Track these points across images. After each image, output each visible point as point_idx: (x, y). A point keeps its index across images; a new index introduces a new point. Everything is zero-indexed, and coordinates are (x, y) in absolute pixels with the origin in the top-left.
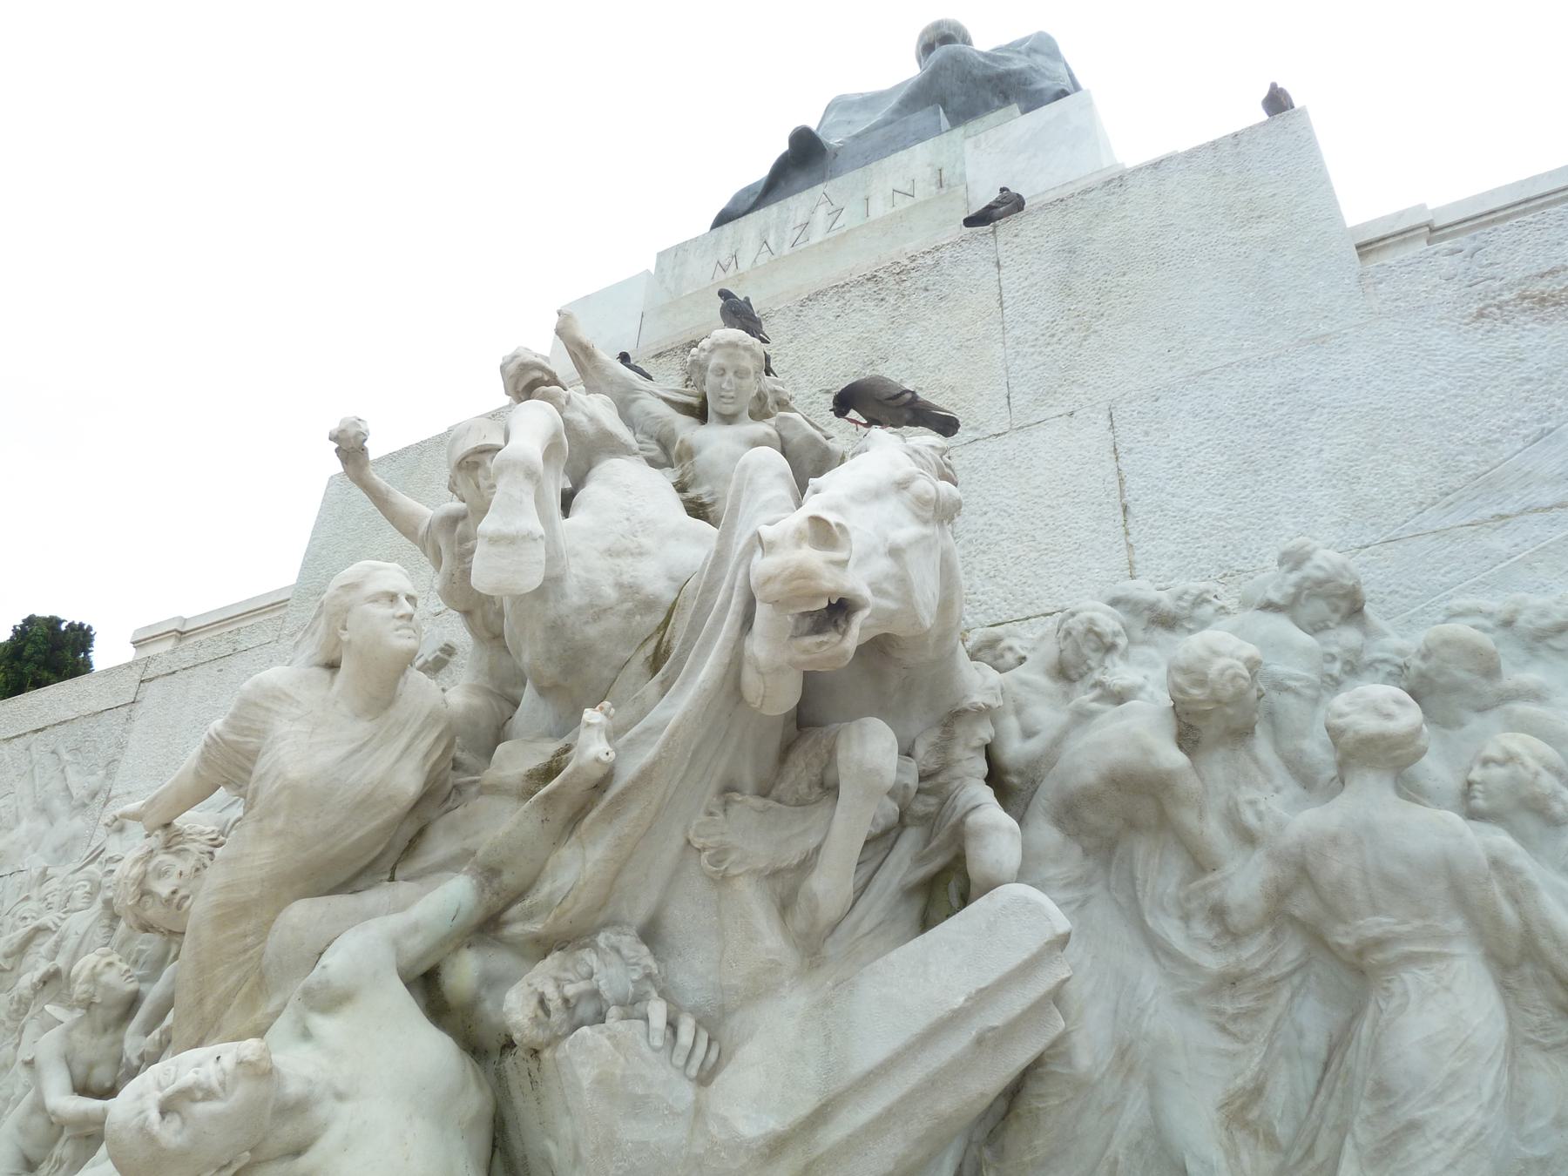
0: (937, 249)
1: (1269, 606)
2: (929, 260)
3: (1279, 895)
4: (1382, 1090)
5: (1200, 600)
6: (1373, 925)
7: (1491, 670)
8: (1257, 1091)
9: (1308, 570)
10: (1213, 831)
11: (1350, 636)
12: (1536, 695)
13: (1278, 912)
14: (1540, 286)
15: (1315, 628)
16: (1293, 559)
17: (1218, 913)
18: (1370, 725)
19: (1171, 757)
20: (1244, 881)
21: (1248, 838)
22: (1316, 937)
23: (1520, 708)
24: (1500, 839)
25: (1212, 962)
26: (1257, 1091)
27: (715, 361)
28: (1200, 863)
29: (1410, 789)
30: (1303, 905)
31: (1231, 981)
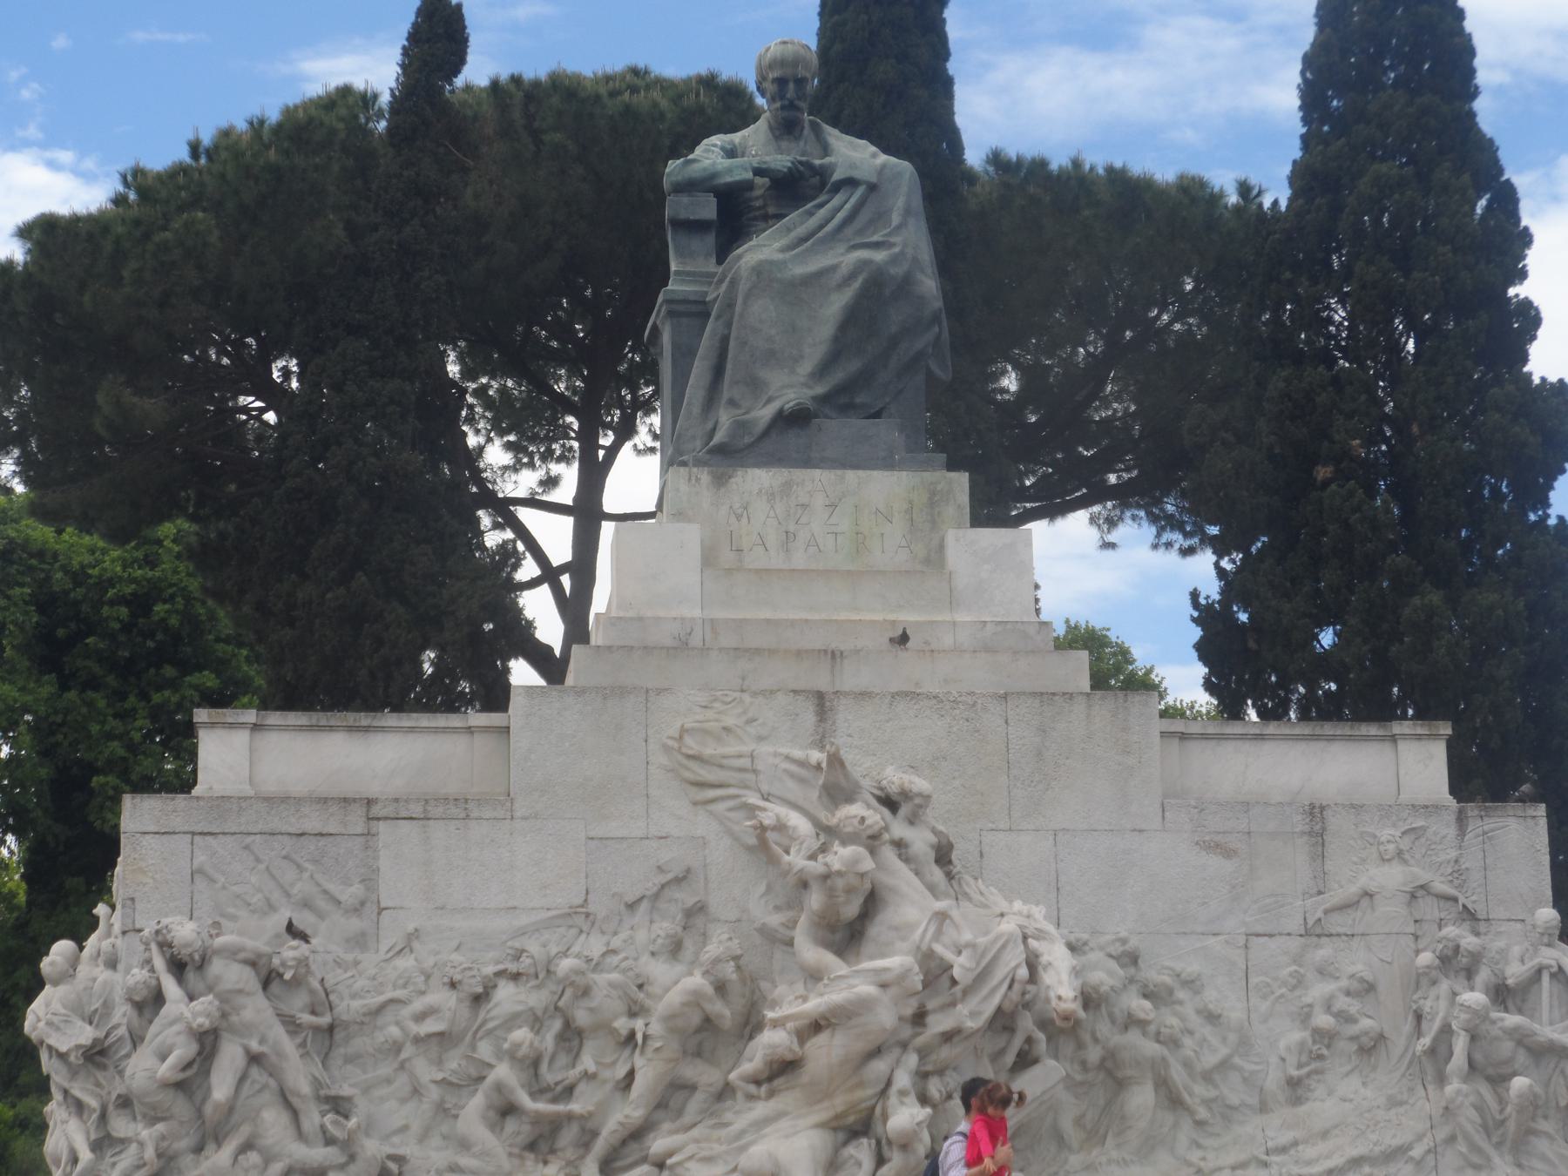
0: (971, 694)
1: (1111, 956)
2: (970, 700)
3: (1103, 1060)
4: (1123, 1118)
5: (1085, 944)
6: (1129, 1072)
7: (1171, 992)
8: (1083, 1116)
9: (1127, 947)
10: (1087, 1037)
11: (1132, 970)
12: (1181, 1003)
13: (1102, 1065)
14: (1218, 838)
15: (1122, 966)
16: (1124, 941)
17: (1083, 1063)
18: (1142, 1016)
19: (1082, 1014)
20: (1094, 1054)
21: (1096, 1040)
22: (1110, 1073)
23: (1178, 1007)
24: (1166, 1052)
25: (1078, 1077)
26: (1083, 1116)
27: (917, 801)
28: (1080, 1046)
29: (1145, 1034)
30: (1109, 1064)
31: (1082, 1084)
